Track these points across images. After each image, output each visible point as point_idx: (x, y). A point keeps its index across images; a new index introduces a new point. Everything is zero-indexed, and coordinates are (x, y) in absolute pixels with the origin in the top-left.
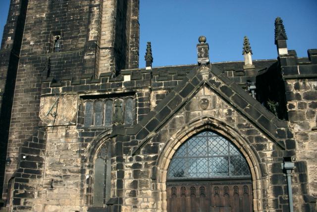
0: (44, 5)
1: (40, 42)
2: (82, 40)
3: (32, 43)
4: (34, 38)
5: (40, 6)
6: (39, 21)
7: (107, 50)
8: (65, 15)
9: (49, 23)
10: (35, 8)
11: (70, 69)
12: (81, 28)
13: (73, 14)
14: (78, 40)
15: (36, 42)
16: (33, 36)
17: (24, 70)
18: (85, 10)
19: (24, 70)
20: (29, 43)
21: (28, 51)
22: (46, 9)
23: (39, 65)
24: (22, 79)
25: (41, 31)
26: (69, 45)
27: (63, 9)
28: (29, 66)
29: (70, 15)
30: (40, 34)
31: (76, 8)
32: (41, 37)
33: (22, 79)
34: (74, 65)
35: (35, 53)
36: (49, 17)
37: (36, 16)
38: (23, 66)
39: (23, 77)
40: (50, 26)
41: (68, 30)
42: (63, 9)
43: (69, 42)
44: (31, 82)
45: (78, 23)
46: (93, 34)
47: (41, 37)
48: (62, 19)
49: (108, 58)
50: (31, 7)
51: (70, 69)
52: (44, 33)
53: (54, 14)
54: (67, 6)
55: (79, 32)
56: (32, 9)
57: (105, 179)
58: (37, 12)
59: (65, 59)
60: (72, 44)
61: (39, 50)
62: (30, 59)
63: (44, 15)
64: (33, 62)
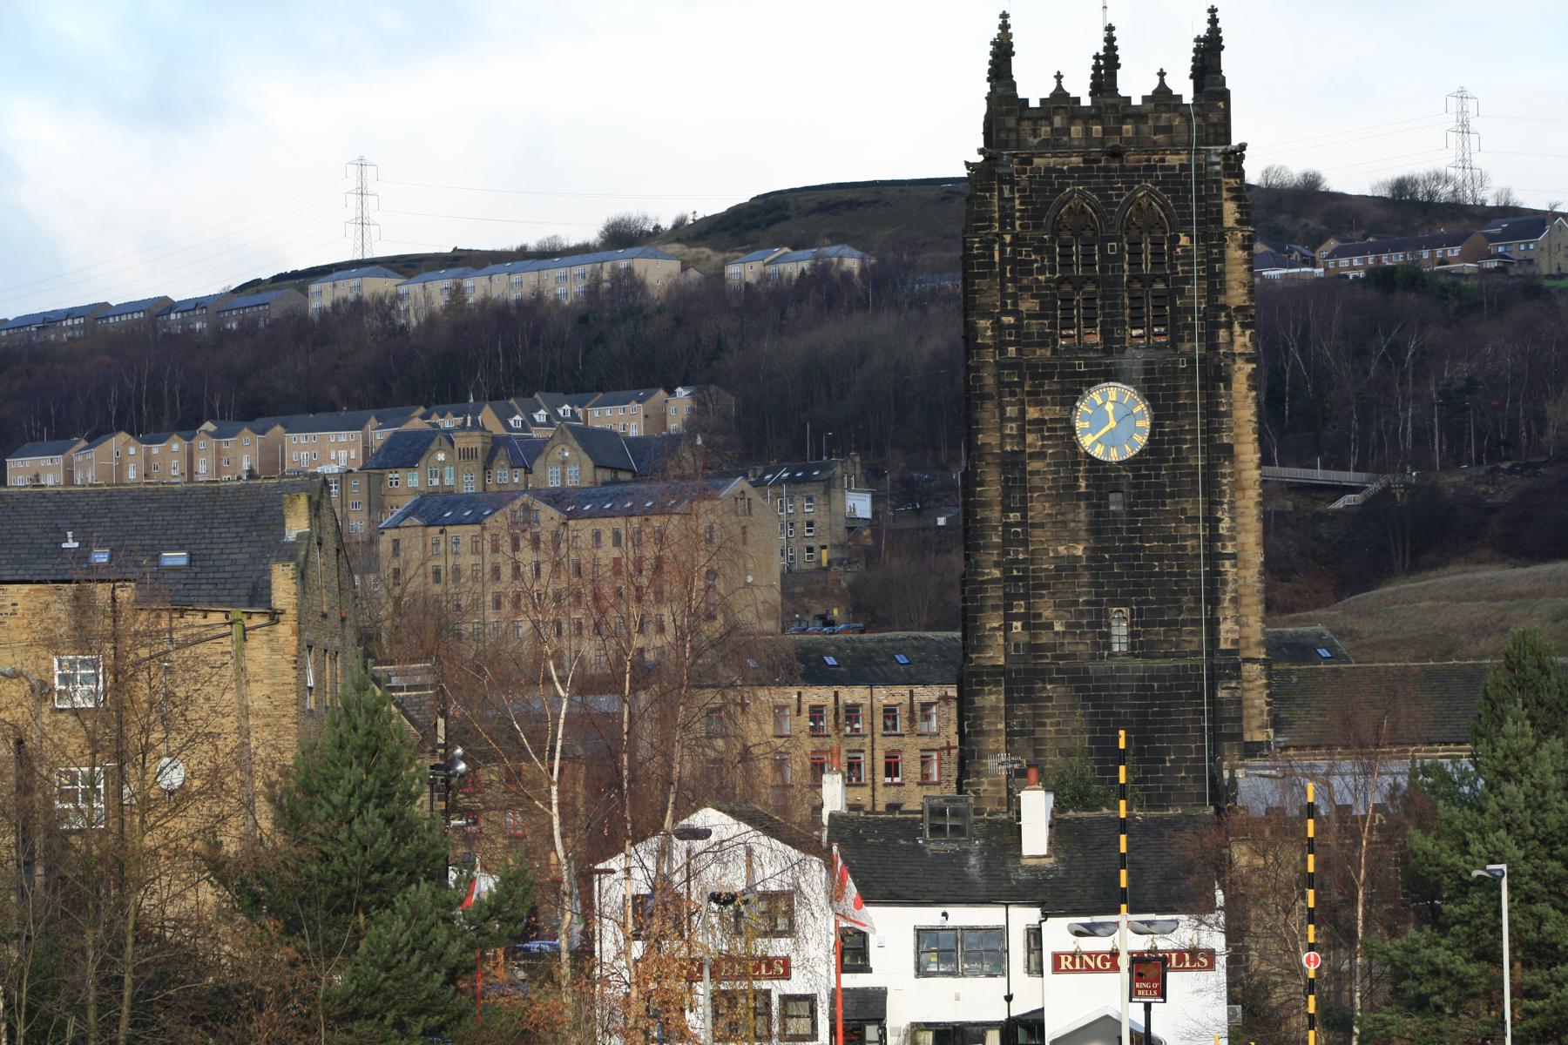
0: (1074, 521)
1: (1080, 626)
2: (1191, 633)
3: (1058, 627)
4: (1061, 613)
5: (1065, 523)
6: (1068, 567)
7: (1257, 667)
8: (1137, 558)
9: (1096, 576)
10: (1050, 525)
11: (1169, 705)
12: (1185, 599)
13: (1160, 558)
14: (1180, 630)
15: (1068, 625)
16: (1057, 606)
17: (1050, 699)
18: (1189, 549)
19: (1050, 699)
20: (1050, 626)
21: (1053, 647)
22: (1083, 534)
23: (1088, 689)
24: (1048, 721)
25: (1079, 595)
26: (1159, 641)
27: (1131, 540)
28: (1061, 689)
29: (1150, 558)
30: (1076, 603)
31: (1166, 539)
32: (1081, 614)
33: (1048, 721)
34: (1179, 696)
35: (1073, 655)
36: (1094, 554)
37: (1056, 551)
38: (1045, 688)
39: (1053, 716)
40: (1102, 585)
41: (1153, 602)
42: (1131, 540)
43: (1158, 633)
44: (1074, 732)
45: (1177, 583)
46: (1227, 631)
47: (1081, 614)
48: (1132, 567)
49: (1260, 686)
50: (1036, 520)
51: (1169, 705)
52: (1087, 603)
53: (1107, 550)
54: (1139, 530)
55: (1181, 613)
56: (1042, 526)
57: (873, 774)
58: (1058, 540)
59: (1153, 678)
60: (1166, 641)
61: (1081, 647)
62: (1059, 671)
63: (1079, 550)
64: (1071, 680)
